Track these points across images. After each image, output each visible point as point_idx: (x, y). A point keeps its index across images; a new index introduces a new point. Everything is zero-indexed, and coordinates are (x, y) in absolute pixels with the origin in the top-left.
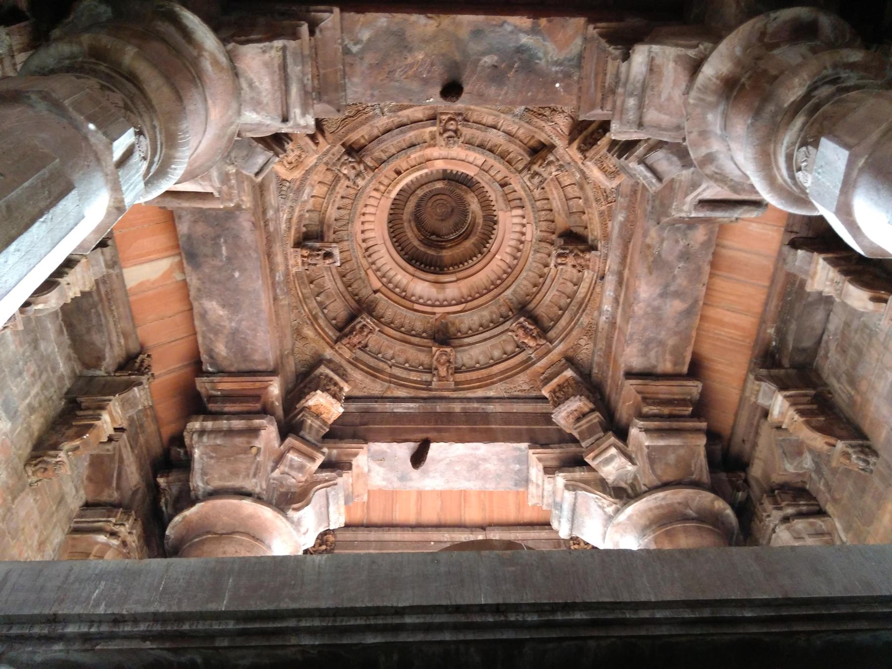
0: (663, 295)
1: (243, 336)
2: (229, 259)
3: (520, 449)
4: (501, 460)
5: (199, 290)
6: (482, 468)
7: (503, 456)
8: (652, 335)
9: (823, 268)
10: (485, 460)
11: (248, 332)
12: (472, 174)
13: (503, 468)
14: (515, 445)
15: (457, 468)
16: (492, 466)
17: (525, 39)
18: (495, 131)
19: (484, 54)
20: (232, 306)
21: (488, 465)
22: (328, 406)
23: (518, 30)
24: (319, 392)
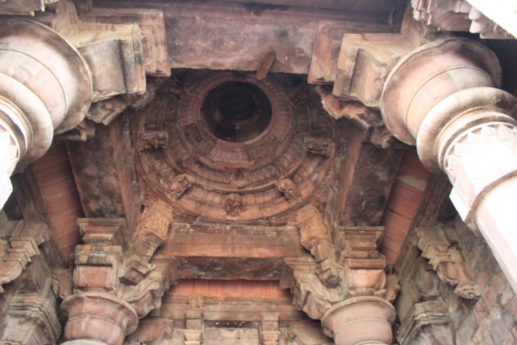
0: (101, 178)
1: (373, 160)
2: (363, 200)
3: (177, 61)
4: (192, 50)
5: (387, 185)
6: (209, 42)
7: (191, 54)
8: (97, 153)
9: (32, 253)
10: (206, 51)
11: (368, 162)
12: (219, 140)
13: (191, 42)
14: (182, 66)
15: (232, 43)
16: (200, 44)
17: (203, 273)
18: (209, 189)
19: (220, 271)
20: (372, 177)
21: (204, 45)
22: (332, 109)
23: (207, 276)
24: (336, 118)
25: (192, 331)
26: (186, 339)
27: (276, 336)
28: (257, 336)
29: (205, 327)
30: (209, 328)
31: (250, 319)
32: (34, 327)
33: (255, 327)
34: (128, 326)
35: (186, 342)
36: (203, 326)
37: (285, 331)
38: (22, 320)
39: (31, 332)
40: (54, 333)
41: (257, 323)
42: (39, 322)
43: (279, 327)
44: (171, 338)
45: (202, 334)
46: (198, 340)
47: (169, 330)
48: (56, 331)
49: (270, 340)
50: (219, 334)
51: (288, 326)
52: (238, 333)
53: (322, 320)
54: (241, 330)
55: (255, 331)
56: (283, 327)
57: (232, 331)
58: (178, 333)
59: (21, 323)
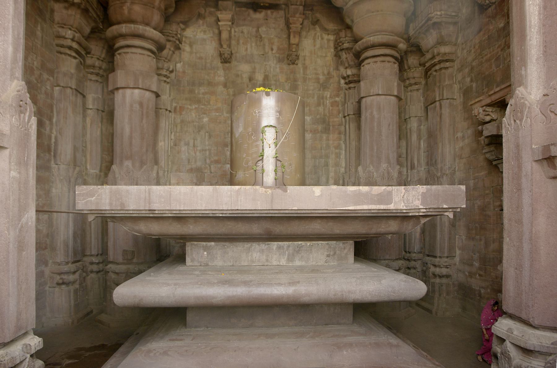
25: (224, 12)
26: (219, 21)
27: (301, 20)
28: (284, 18)
29: (235, 8)
30: (237, 9)
31: (278, 2)
32: (79, 11)
33: (281, 9)
34: (166, 9)
35: (219, 23)
36: (234, 7)
37: (309, 14)
38: (66, 5)
39: (78, 16)
40: (98, 16)
41: (283, 6)
42: (82, 6)
43: (304, 10)
44: (204, 18)
45: (233, 16)
46: (230, 21)
47: (202, 11)
48: (99, 13)
49: (295, 23)
50: (249, 15)
51: (312, 10)
52: (266, 15)
53: (345, 8)
54: (269, 12)
55: (282, 13)
56: (307, 10)
57: (260, 12)
58: (211, 13)
59: (66, 8)
